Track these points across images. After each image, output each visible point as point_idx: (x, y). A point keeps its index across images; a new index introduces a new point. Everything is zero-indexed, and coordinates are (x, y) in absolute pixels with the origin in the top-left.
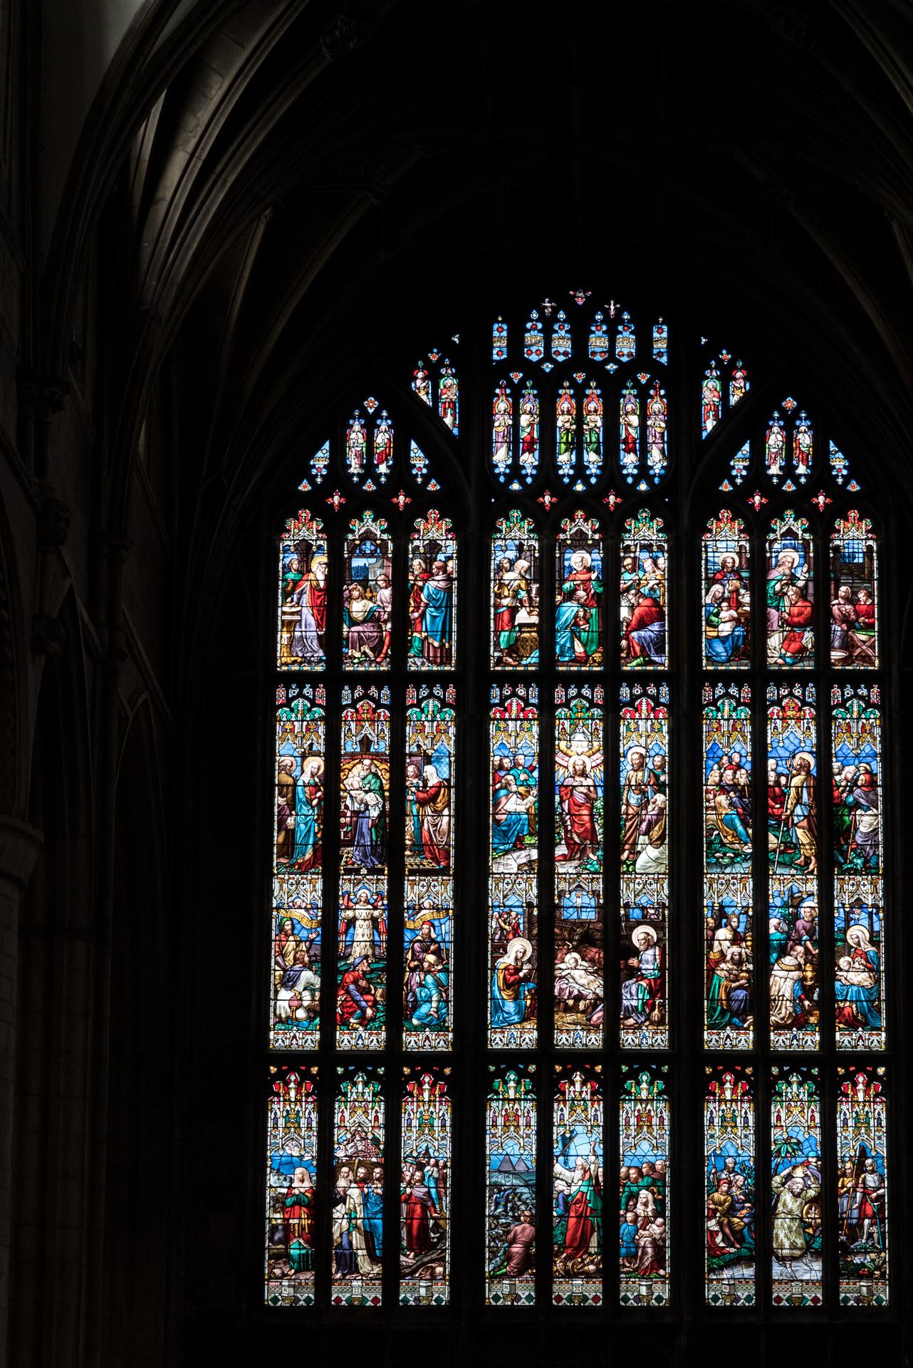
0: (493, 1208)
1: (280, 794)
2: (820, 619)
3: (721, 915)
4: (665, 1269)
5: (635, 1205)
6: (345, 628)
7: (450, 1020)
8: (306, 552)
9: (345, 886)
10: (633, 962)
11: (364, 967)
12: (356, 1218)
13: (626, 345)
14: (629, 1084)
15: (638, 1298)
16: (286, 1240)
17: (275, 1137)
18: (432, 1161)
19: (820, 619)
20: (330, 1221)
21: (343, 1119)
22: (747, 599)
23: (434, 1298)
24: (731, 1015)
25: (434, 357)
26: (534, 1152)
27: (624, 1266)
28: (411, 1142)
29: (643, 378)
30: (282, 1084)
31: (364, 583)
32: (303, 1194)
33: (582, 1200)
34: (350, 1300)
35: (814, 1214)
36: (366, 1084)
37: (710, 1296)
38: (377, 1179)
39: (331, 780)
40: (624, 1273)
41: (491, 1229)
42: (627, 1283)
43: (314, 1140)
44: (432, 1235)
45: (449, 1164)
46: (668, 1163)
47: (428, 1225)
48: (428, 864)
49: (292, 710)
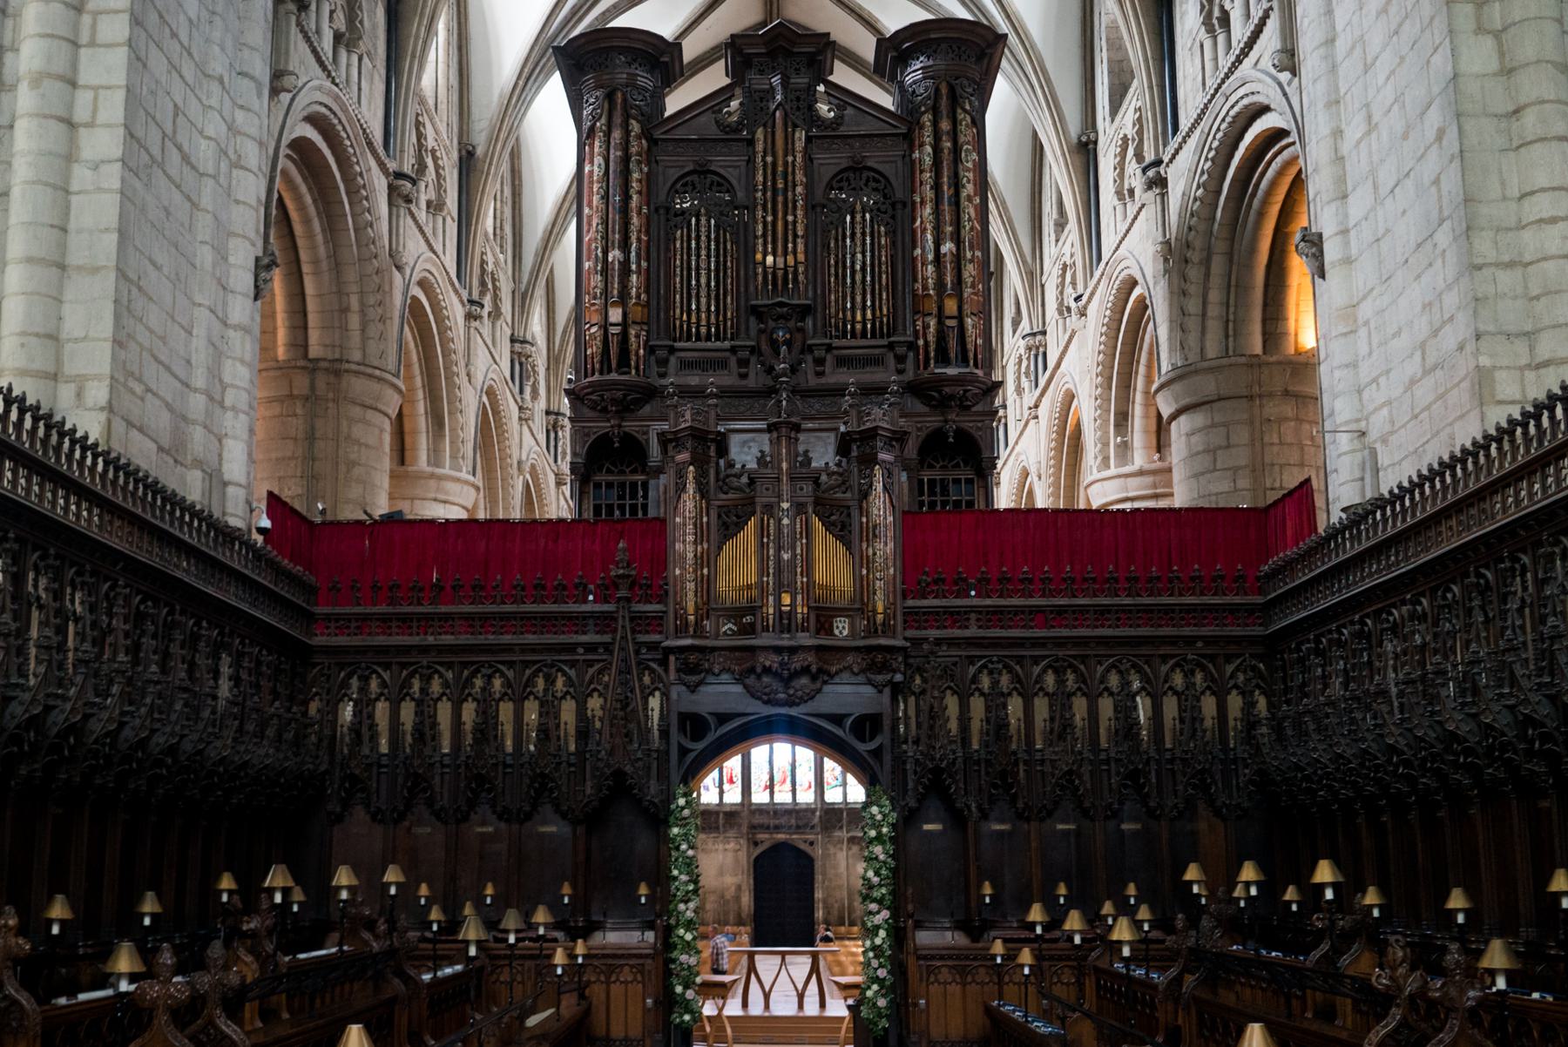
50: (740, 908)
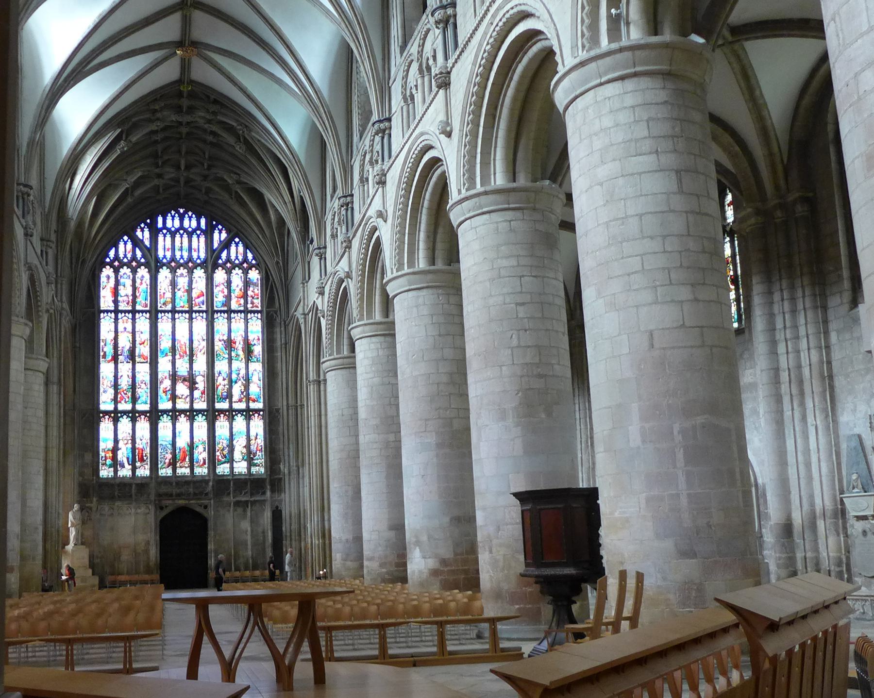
2: (245, 296)
3: (220, 373)
7: (149, 402)
8: (108, 277)
9: (120, 365)
10: (197, 386)
11: (125, 388)
13: (194, 224)
14: (196, 417)
16: (106, 460)
19: (245, 296)
22: (226, 291)
24: (223, 399)
25: (142, 225)
29: (198, 232)
31: (124, 286)
33: (184, 448)
35: (244, 450)
39: (116, 338)
48: (142, 360)
50: (148, 558)
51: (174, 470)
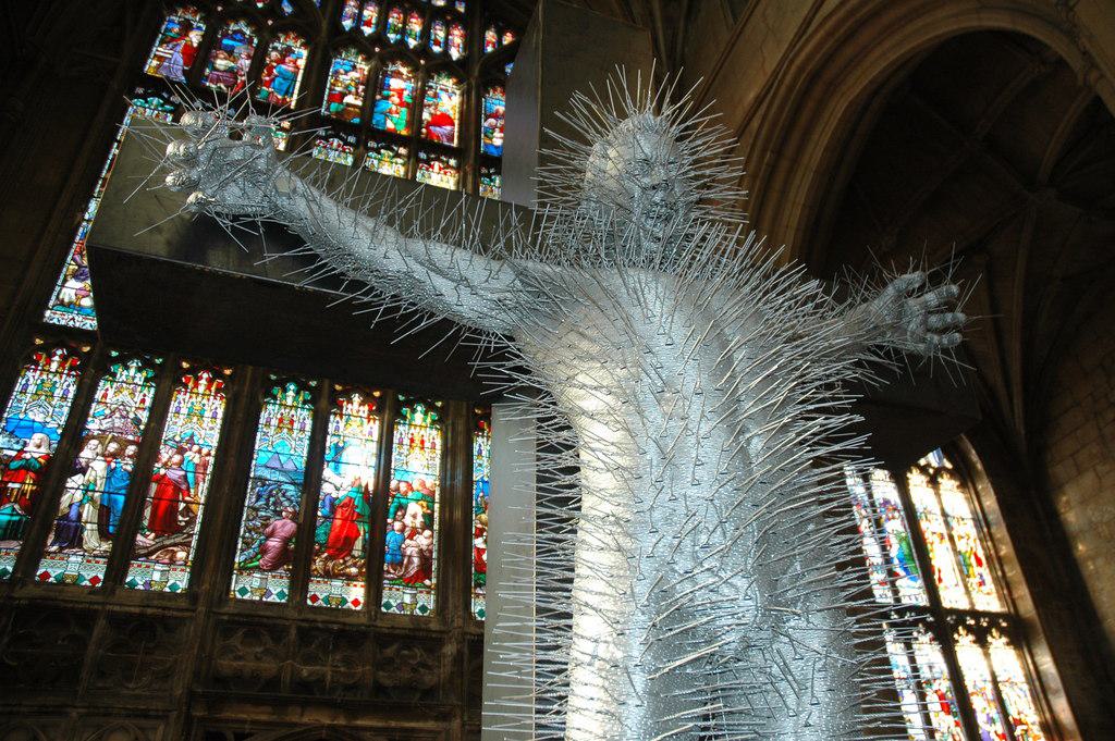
0: (253, 500)
1: (117, 148)
4: (430, 579)
5: (404, 516)
6: (208, 70)
12: (94, 491)
15: (401, 606)
17: (20, 401)
18: (196, 448)
20: (61, 489)
21: (105, 396)
23: (169, 584)
26: (305, 454)
27: (389, 572)
28: (175, 427)
30: (44, 356)
32: (36, 459)
33: (349, 503)
34: (61, 581)
36: (139, 370)
37: (477, 611)
38: (129, 456)
40: (388, 579)
41: (248, 520)
42: (390, 589)
43: (66, 410)
44: (180, 518)
45: (213, 453)
46: (438, 483)
47: (177, 507)
49: (147, 102)
51: (299, 583)
